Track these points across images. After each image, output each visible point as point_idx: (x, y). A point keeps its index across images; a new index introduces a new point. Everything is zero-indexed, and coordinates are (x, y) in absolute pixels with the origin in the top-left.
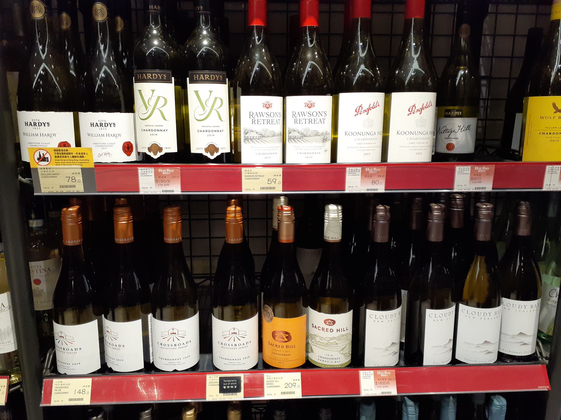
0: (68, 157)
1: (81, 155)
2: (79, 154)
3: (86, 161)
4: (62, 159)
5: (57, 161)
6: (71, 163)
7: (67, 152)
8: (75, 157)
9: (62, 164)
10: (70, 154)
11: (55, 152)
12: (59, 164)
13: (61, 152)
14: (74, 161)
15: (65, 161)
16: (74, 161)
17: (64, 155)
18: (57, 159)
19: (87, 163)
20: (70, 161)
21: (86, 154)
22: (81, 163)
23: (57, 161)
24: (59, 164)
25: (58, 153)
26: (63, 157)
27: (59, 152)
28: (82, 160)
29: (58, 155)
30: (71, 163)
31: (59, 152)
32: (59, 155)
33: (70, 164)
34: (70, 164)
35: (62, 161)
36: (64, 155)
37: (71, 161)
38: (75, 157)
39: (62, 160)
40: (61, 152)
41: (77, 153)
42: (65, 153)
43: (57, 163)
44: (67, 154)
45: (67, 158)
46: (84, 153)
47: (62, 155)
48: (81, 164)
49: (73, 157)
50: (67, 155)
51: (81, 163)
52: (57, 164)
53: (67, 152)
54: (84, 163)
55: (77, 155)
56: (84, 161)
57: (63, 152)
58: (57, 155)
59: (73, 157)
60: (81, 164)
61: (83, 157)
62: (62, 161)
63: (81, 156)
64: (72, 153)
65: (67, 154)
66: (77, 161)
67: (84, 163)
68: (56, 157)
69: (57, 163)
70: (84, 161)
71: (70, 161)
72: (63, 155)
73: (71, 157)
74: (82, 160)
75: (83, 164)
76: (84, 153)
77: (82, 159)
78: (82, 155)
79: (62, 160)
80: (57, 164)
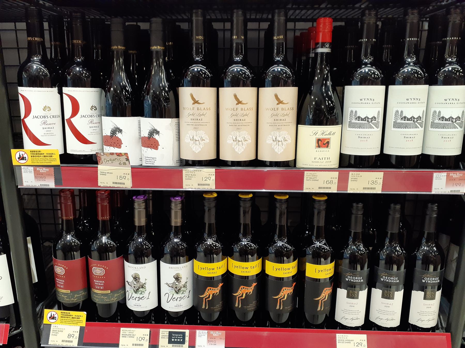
0: (41, 156)
1: (51, 155)
2: (49, 154)
3: (54, 160)
4: (36, 158)
5: (32, 160)
6: (43, 161)
7: (40, 153)
8: (46, 156)
9: (37, 162)
10: (42, 154)
11: (31, 153)
12: (33, 162)
13: (36, 153)
14: (45, 160)
15: (39, 160)
16: (45, 160)
17: (38, 155)
18: (33, 158)
19: (55, 161)
20: (42, 160)
21: (54, 154)
22: (50, 161)
23: (32, 160)
24: (33, 162)
25: (33, 154)
26: (37, 156)
27: (34, 153)
28: (50, 159)
29: (33, 155)
30: (43, 161)
31: (34, 153)
32: (34, 155)
33: (42, 162)
34: (42, 162)
35: (36, 160)
36: (38, 155)
37: (43, 160)
38: (46, 156)
39: (36, 159)
40: (36, 153)
41: (47, 154)
42: (38, 154)
43: (32, 161)
44: (40, 154)
45: (40, 158)
46: (53, 154)
47: (36, 155)
48: (50, 162)
49: (44, 156)
50: (40, 155)
51: (50, 161)
52: (32, 162)
53: (40, 153)
54: (52, 161)
55: (47, 155)
56: (53, 160)
57: (37, 153)
58: (32, 155)
59: (44, 156)
60: (50, 162)
61: (52, 156)
62: (36, 160)
63: (50, 156)
64: (44, 154)
65: (40, 154)
66: (47, 160)
67: (52, 161)
68: (31, 156)
69: (32, 161)
70: (53, 160)
71: (42, 160)
72: (37, 155)
73: (43, 156)
74: (50, 159)
75: (51, 162)
76: (53, 154)
77: (51, 158)
78: (51, 155)
79: (36, 159)
80: (32, 162)
